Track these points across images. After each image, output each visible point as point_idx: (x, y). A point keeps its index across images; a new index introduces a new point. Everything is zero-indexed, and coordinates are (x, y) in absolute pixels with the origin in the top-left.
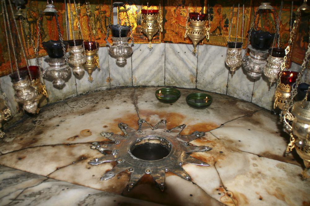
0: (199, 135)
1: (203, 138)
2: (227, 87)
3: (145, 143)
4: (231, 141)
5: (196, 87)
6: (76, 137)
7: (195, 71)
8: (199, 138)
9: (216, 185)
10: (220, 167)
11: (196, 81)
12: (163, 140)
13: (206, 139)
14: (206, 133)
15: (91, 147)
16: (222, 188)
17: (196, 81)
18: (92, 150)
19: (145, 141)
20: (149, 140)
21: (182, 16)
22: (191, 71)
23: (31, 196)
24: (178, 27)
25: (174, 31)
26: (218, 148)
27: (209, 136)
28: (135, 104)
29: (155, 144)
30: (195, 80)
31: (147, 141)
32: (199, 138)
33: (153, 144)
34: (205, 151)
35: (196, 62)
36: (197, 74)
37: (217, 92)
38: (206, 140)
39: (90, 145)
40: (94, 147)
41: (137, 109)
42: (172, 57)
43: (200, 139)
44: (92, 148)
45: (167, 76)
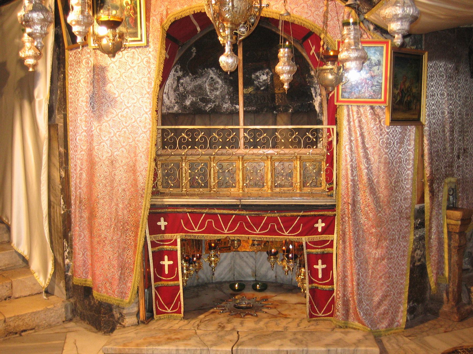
2: (276, 277)
4: (282, 301)
6: (202, 306)
7: (254, 268)
9: (278, 313)
11: (256, 275)
16: (280, 313)
17: (256, 275)
22: (251, 268)
23: (206, 321)
26: (275, 303)
27: (270, 300)
28: (222, 291)
30: (254, 275)
35: (254, 263)
37: (269, 281)
41: (224, 293)
42: (238, 261)
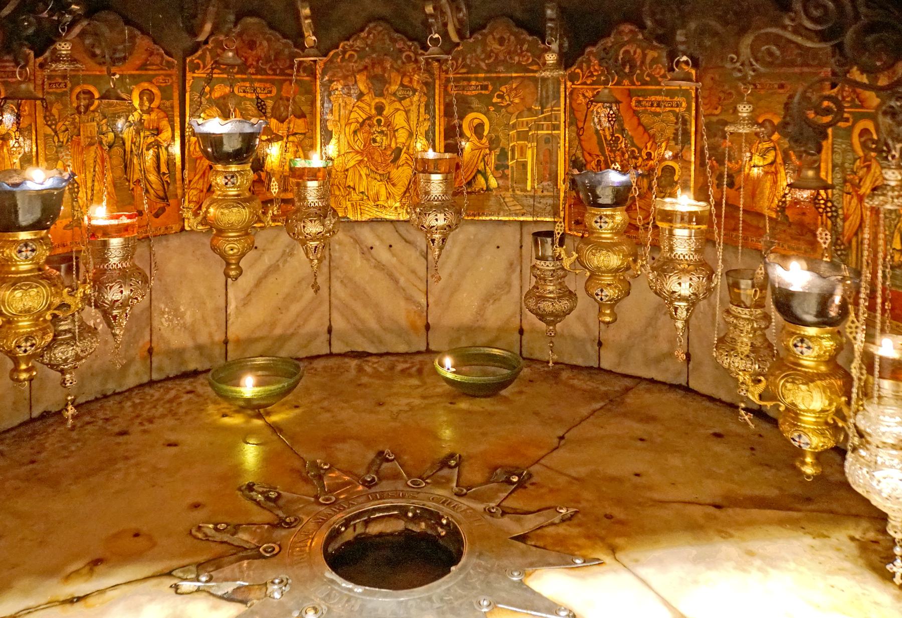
0: (519, 475)
1: (533, 484)
3: (356, 538)
5: (428, 344)
8: (521, 485)
10: (637, 561)
12: (415, 515)
13: (542, 487)
14: (532, 469)
15: (176, 587)
17: (428, 327)
18: (179, 597)
19: (355, 530)
20: (366, 523)
21: (377, 144)
24: (368, 176)
25: (354, 189)
29: (392, 534)
31: (360, 530)
32: (521, 485)
33: (381, 535)
34: (563, 521)
36: (428, 306)
38: (543, 491)
39: (174, 581)
40: (186, 586)
43: (525, 488)
44: (179, 591)
45: (339, 323)
